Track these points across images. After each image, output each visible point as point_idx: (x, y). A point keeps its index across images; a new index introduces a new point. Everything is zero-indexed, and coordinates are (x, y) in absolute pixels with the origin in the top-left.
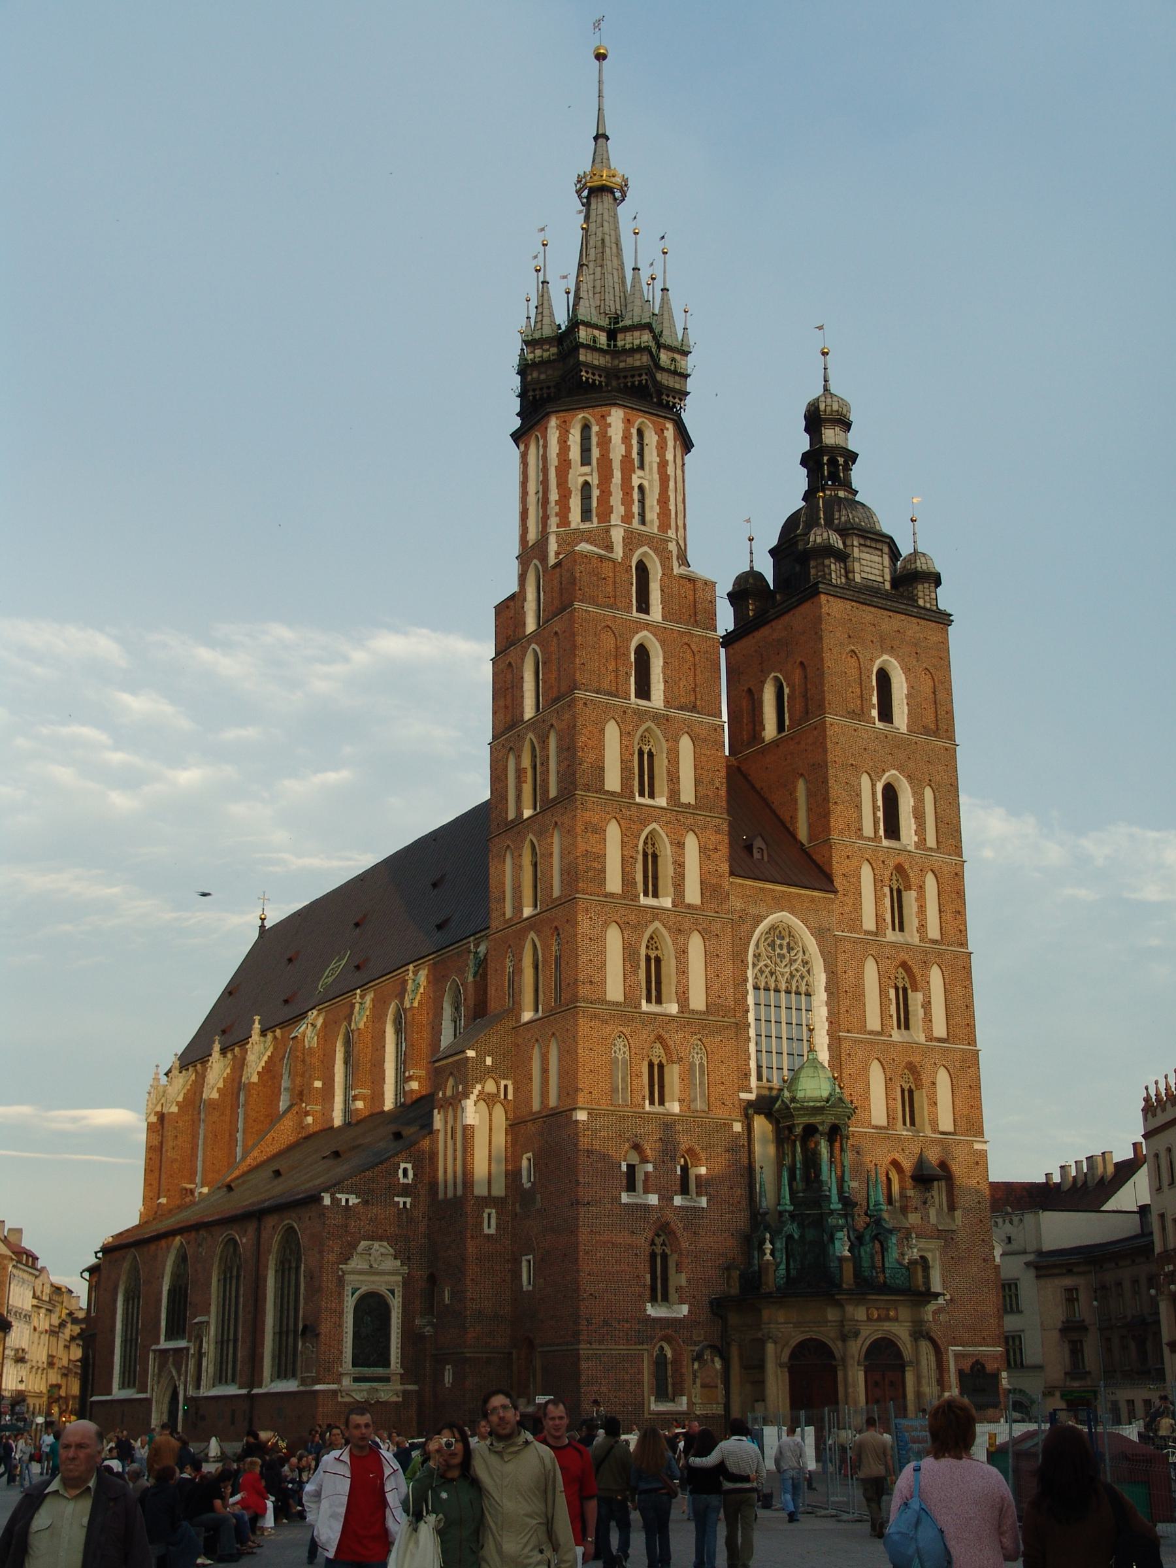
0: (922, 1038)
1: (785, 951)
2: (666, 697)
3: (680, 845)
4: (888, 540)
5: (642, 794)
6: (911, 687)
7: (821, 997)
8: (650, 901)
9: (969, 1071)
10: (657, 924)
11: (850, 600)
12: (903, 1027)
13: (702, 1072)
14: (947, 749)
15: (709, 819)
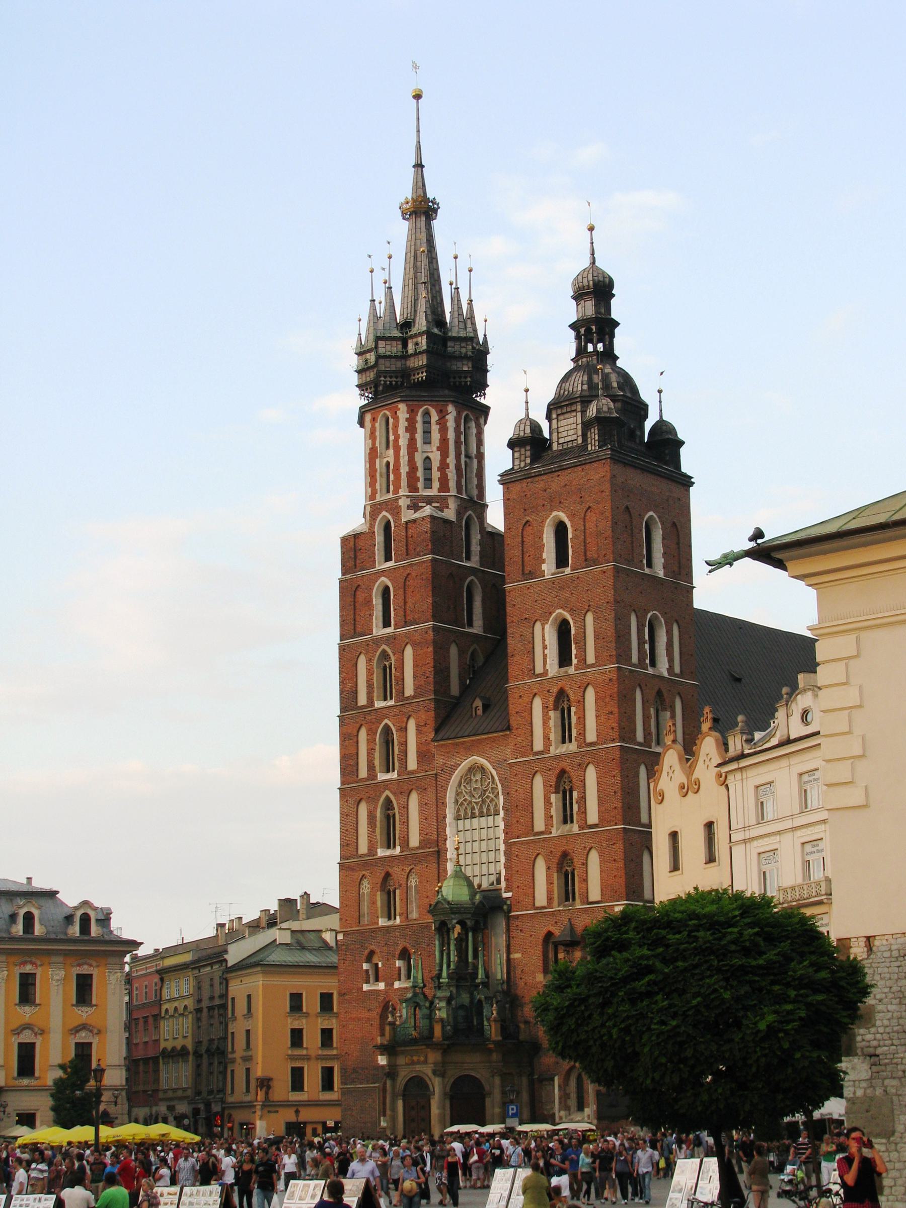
0: (575, 828)
1: (479, 785)
2: (395, 622)
3: (404, 730)
4: (579, 400)
5: (385, 699)
6: (575, 530)
7: (502, 813)
8: (388, 776)
9: (614, 847)
10: (387, 793)
11: (525, 478)
12: (569, 822)
13: (417, 892)
14: (604, 572)
15: (421, 703)
